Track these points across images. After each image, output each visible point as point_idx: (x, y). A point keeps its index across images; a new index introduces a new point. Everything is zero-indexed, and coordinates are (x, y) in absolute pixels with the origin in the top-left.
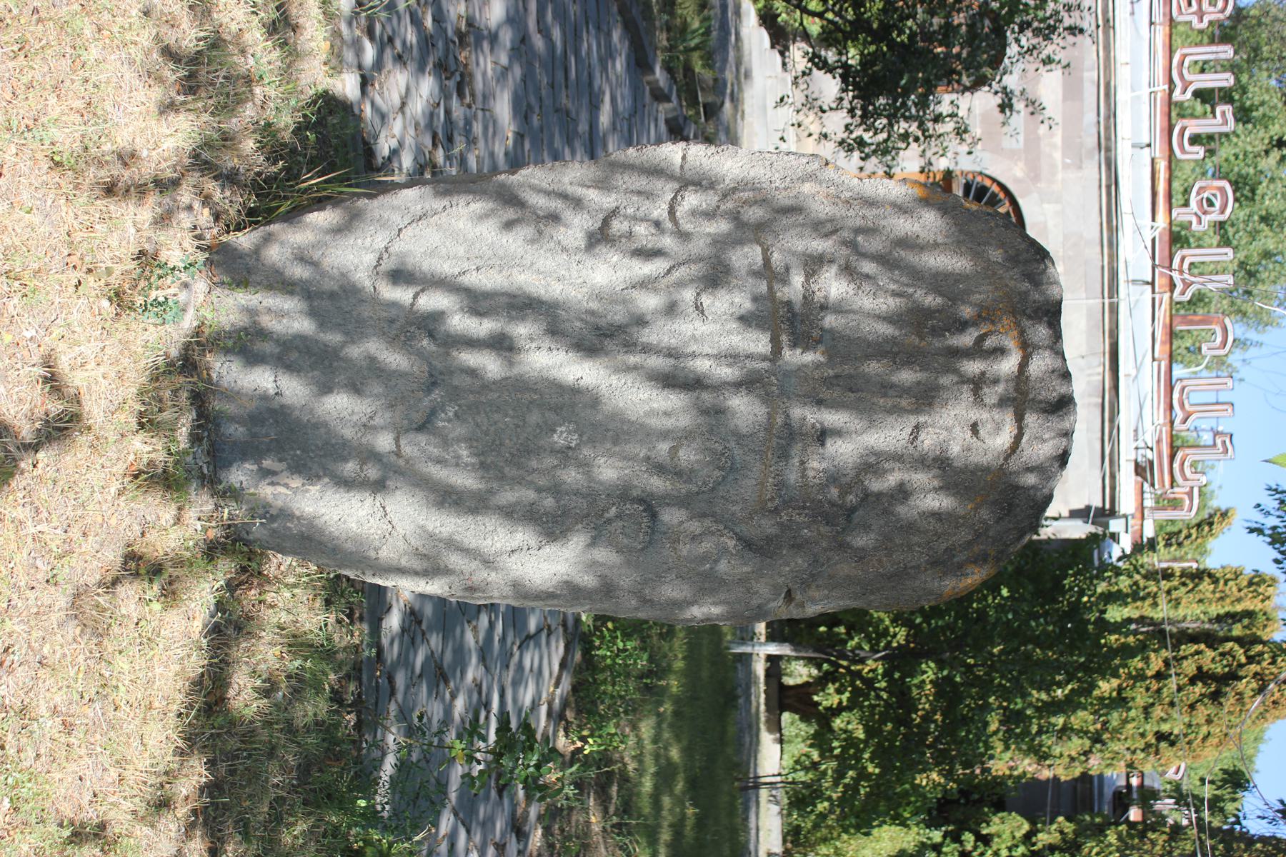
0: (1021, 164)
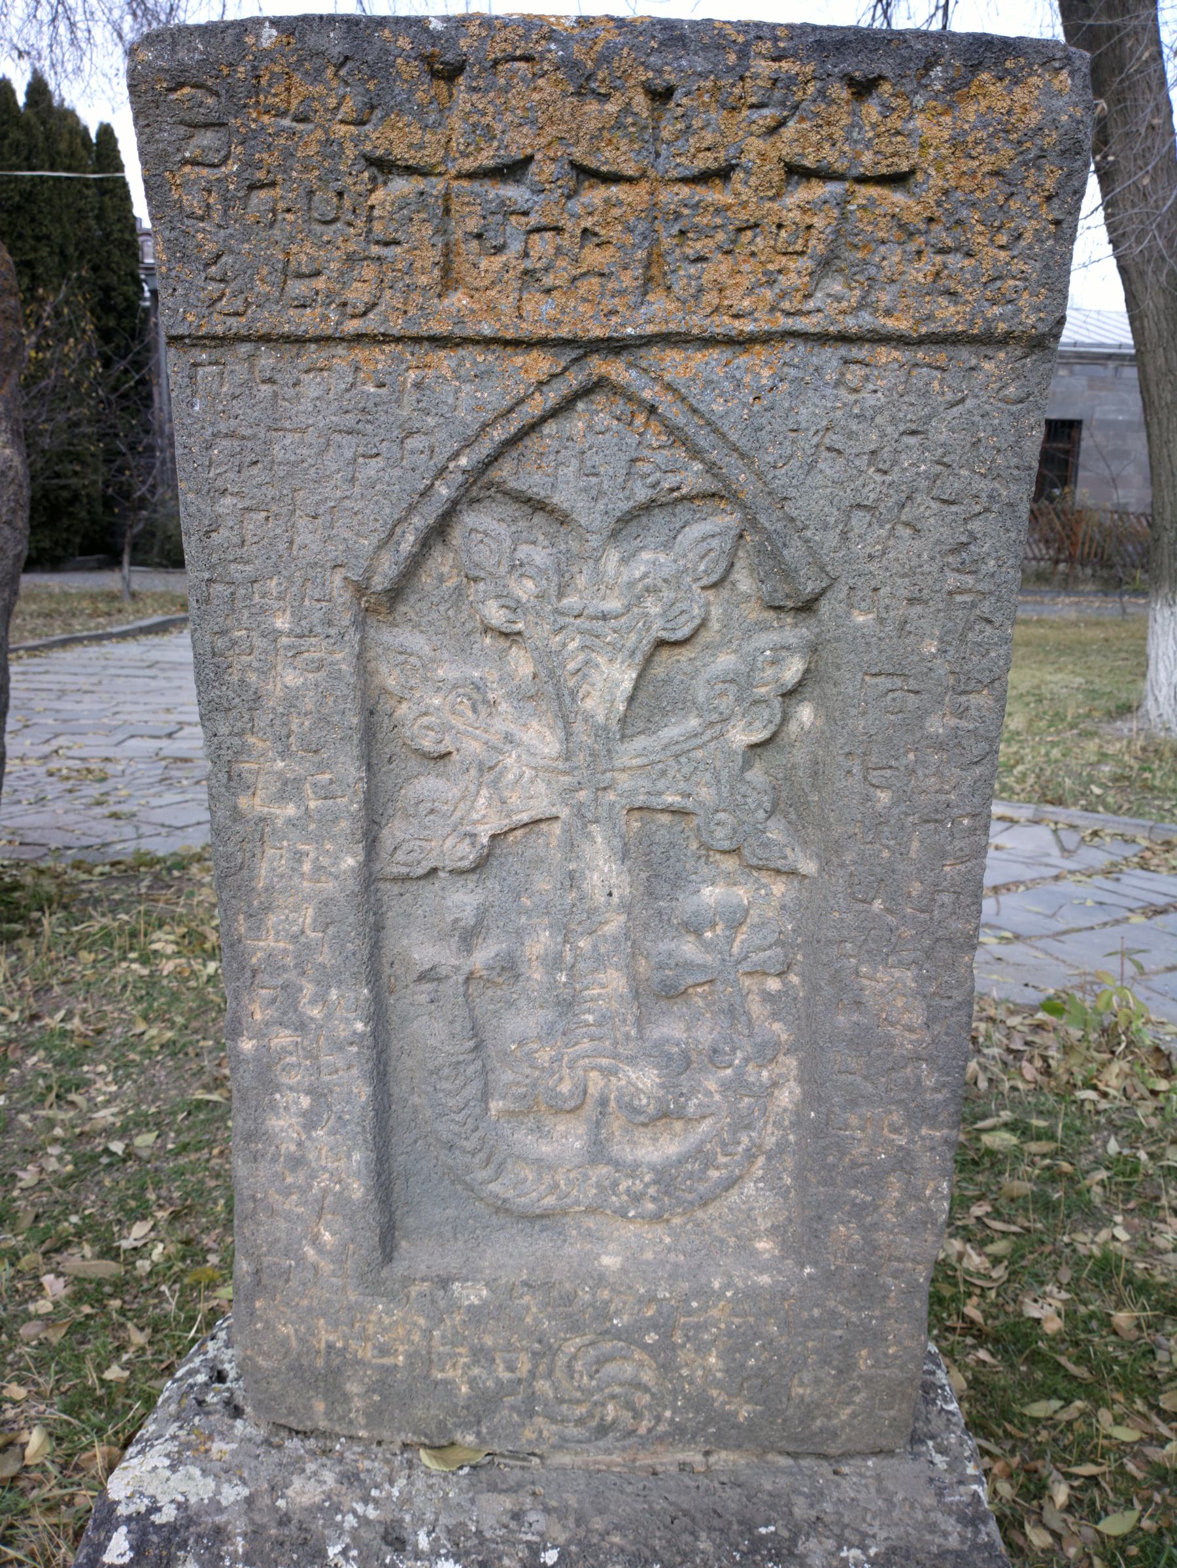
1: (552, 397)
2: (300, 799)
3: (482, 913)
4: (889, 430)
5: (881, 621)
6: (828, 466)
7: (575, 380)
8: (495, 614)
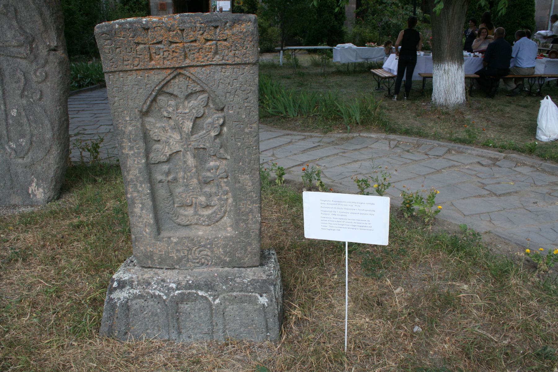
1: (171, 76)
2: (133, 150)
3: (169, 169)
5: (234, 112)
7: (175, 73)
8: (165, 114)
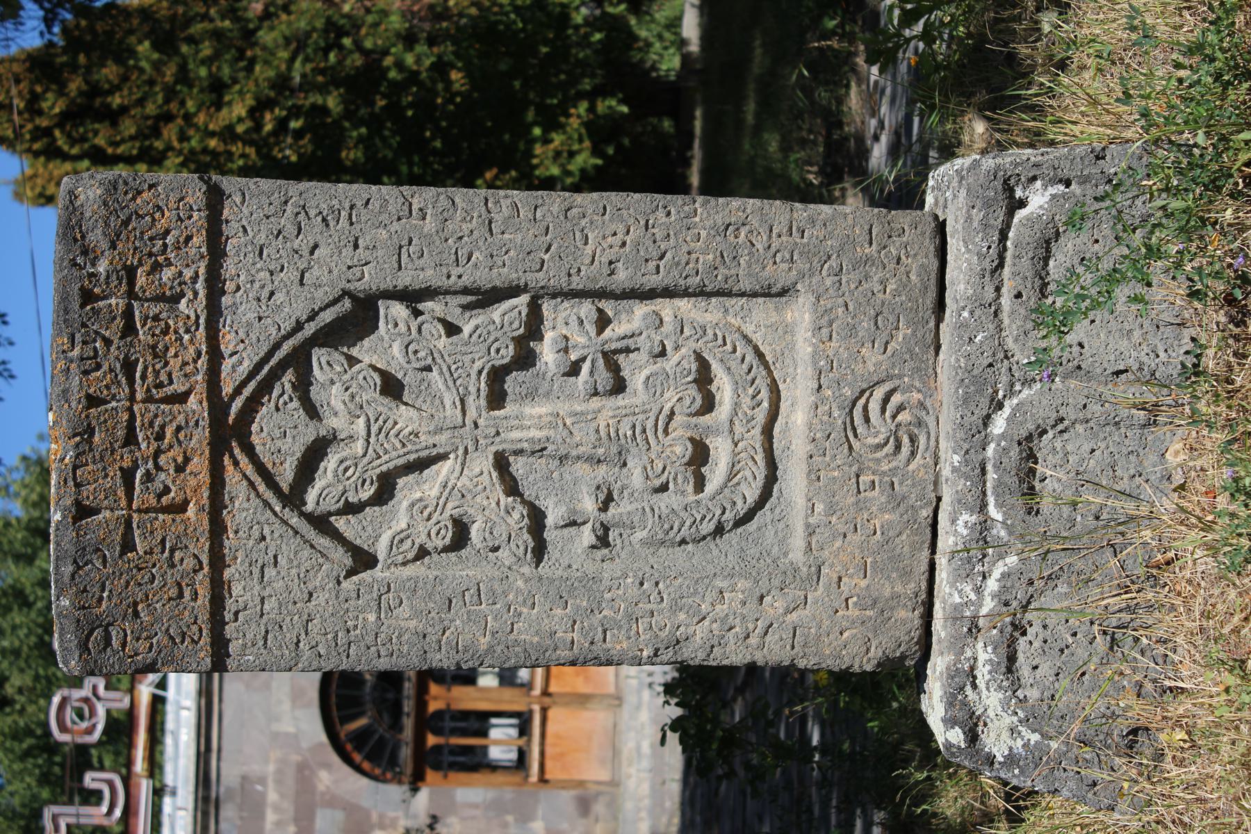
0: (321, 787)
4: (258, 266)
6: (279, 297)
8: (367, 493)
